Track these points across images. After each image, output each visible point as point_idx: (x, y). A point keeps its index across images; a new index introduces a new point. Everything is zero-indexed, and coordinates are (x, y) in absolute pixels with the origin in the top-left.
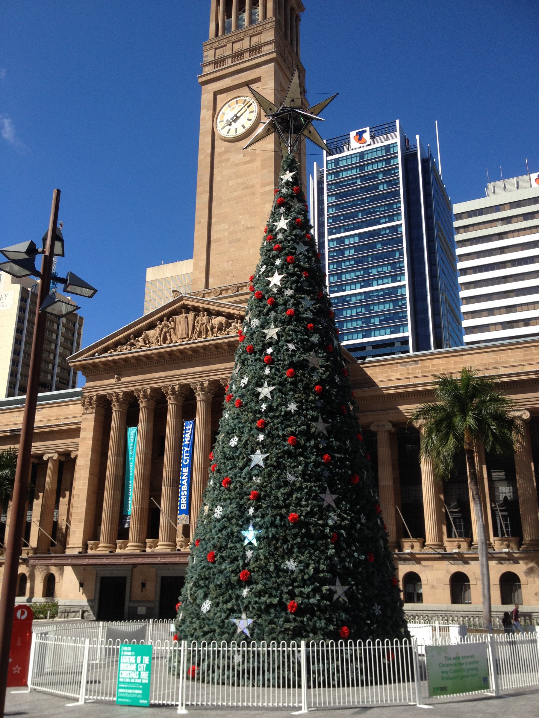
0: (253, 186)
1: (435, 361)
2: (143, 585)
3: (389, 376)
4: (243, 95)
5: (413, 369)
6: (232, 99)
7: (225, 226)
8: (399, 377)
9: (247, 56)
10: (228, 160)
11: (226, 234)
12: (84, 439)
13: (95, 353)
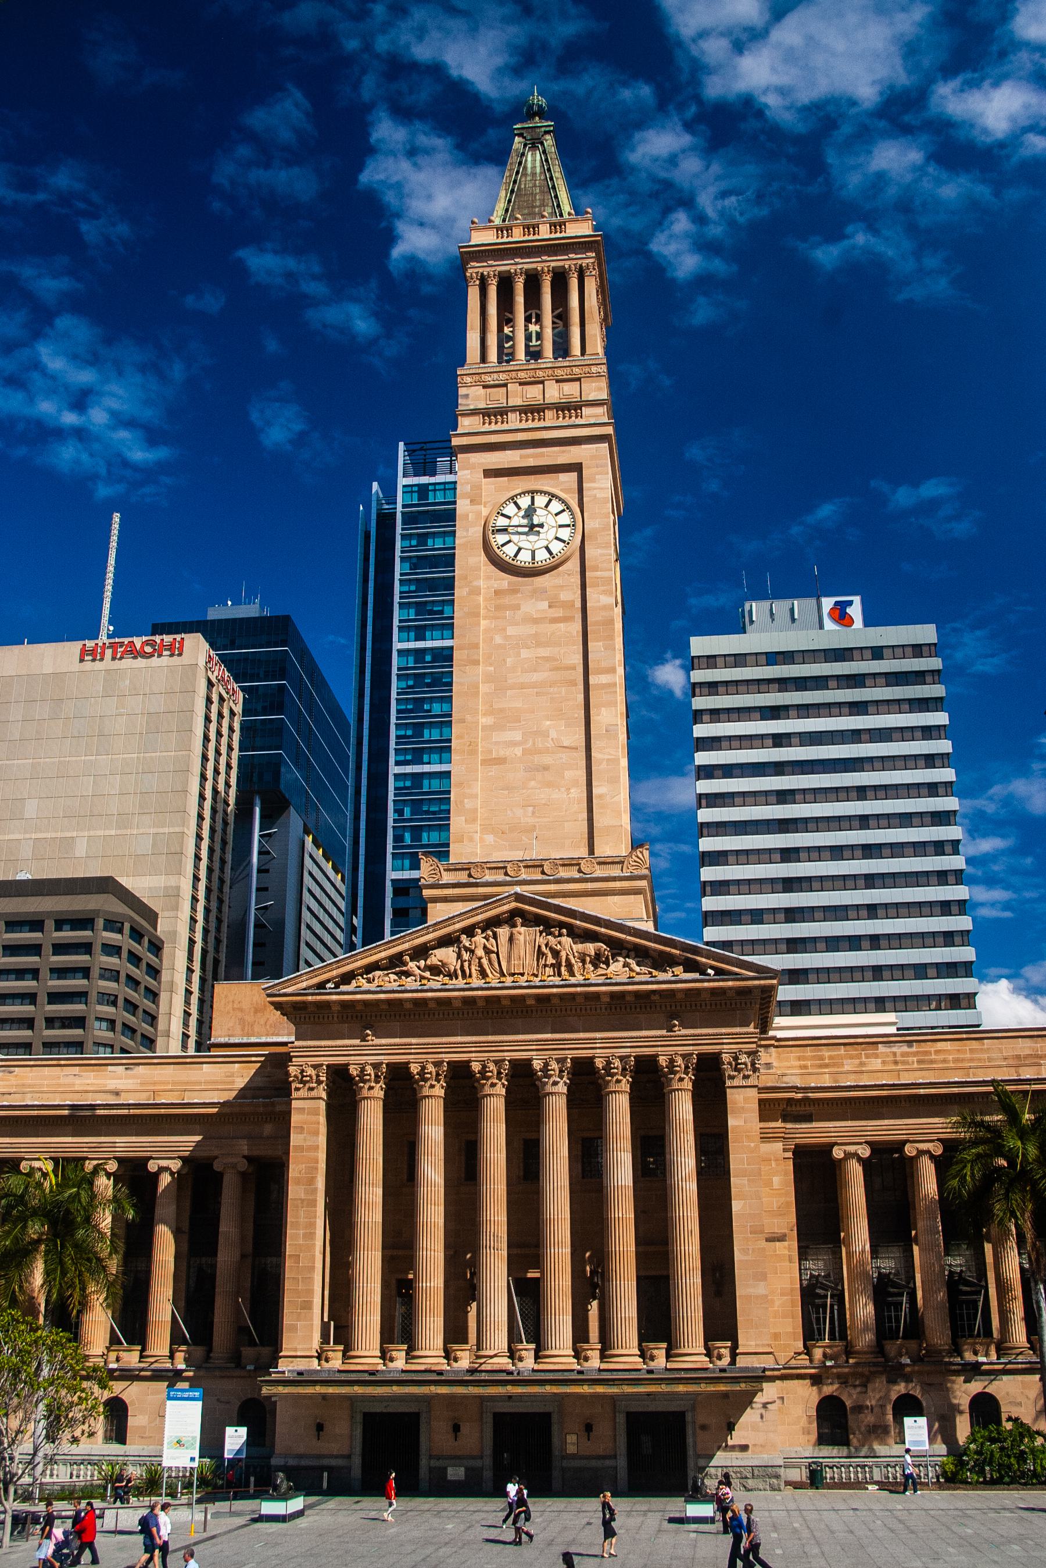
0: (574, 668)
1: (940, 1045)
2: (456, 1428)
3: (862, 1064)
4: (546, 488)
5: (903, 1054)
6: (524, 493)
7: (517, 736)
8: (879, 1067)
9: (550, 418)
10: (517, 607)
11: (518, 751)
12: (300, 1149)
13: (328, 981)
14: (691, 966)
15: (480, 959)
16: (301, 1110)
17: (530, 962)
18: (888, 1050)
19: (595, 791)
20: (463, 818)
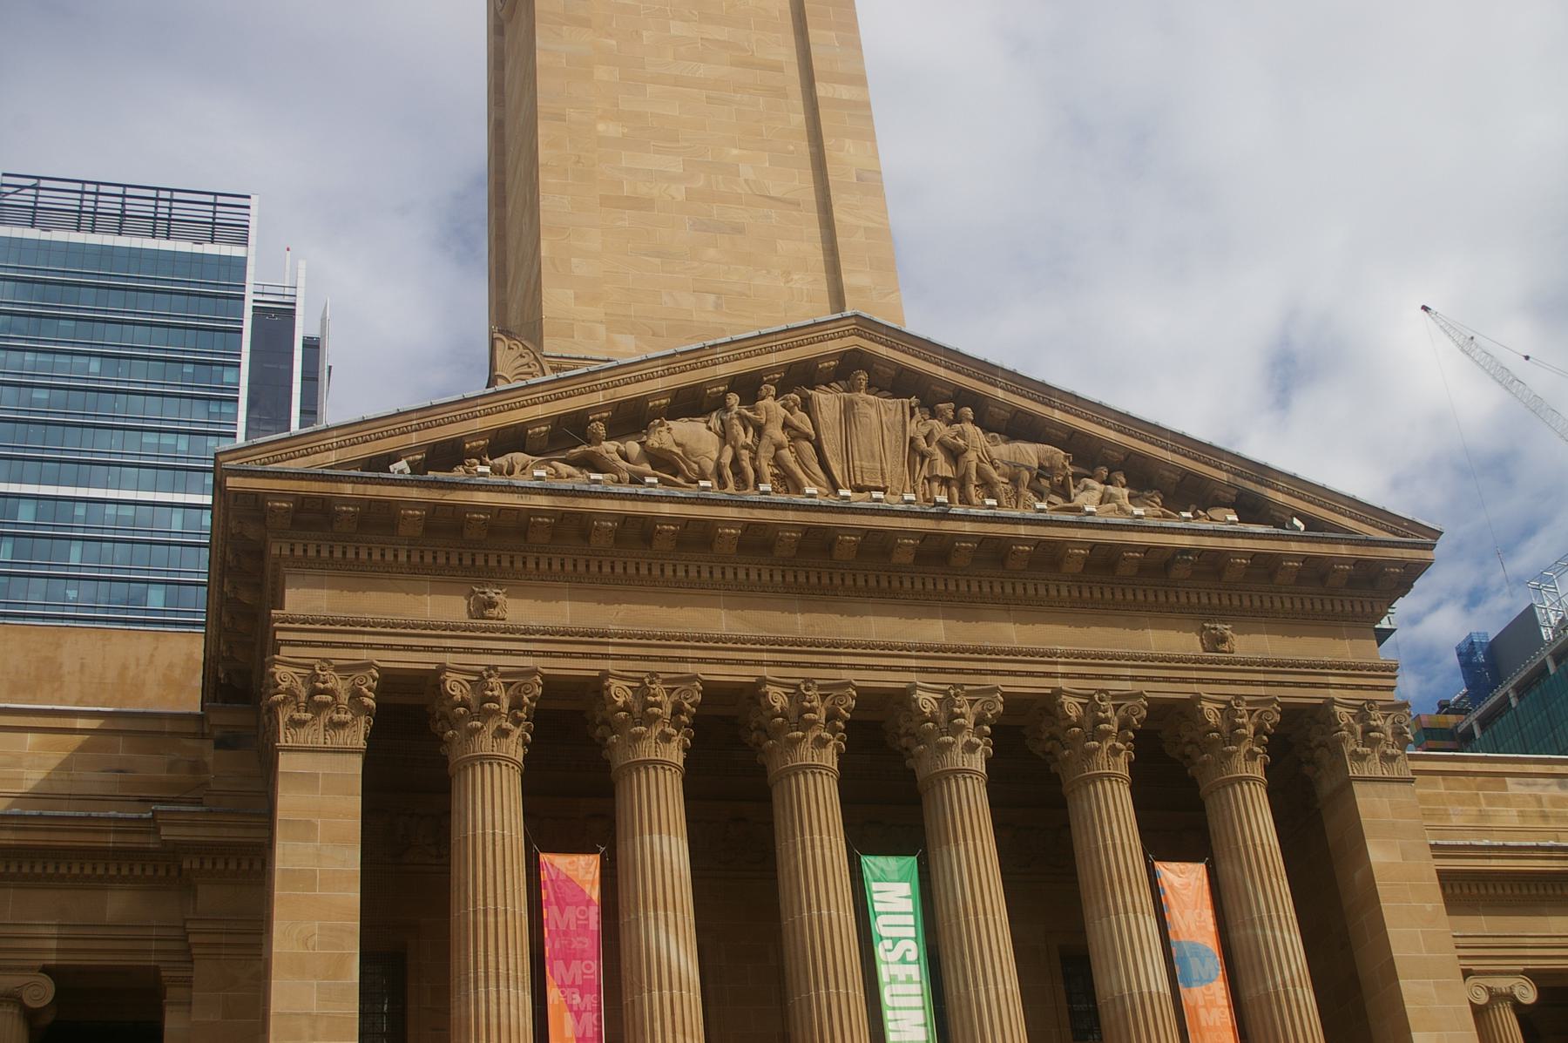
0: (778, 68)
3: (1482, 815)
8: (1516, 822)
11: (678, 192)
12: (305, 879)
13: (393, 457)
14: (1251, 508)
15: (779, 447)
16: (308, 780)
17: (894, 466)
18: (1525, 791)
19: (847, 279)
20: (571, 293)
